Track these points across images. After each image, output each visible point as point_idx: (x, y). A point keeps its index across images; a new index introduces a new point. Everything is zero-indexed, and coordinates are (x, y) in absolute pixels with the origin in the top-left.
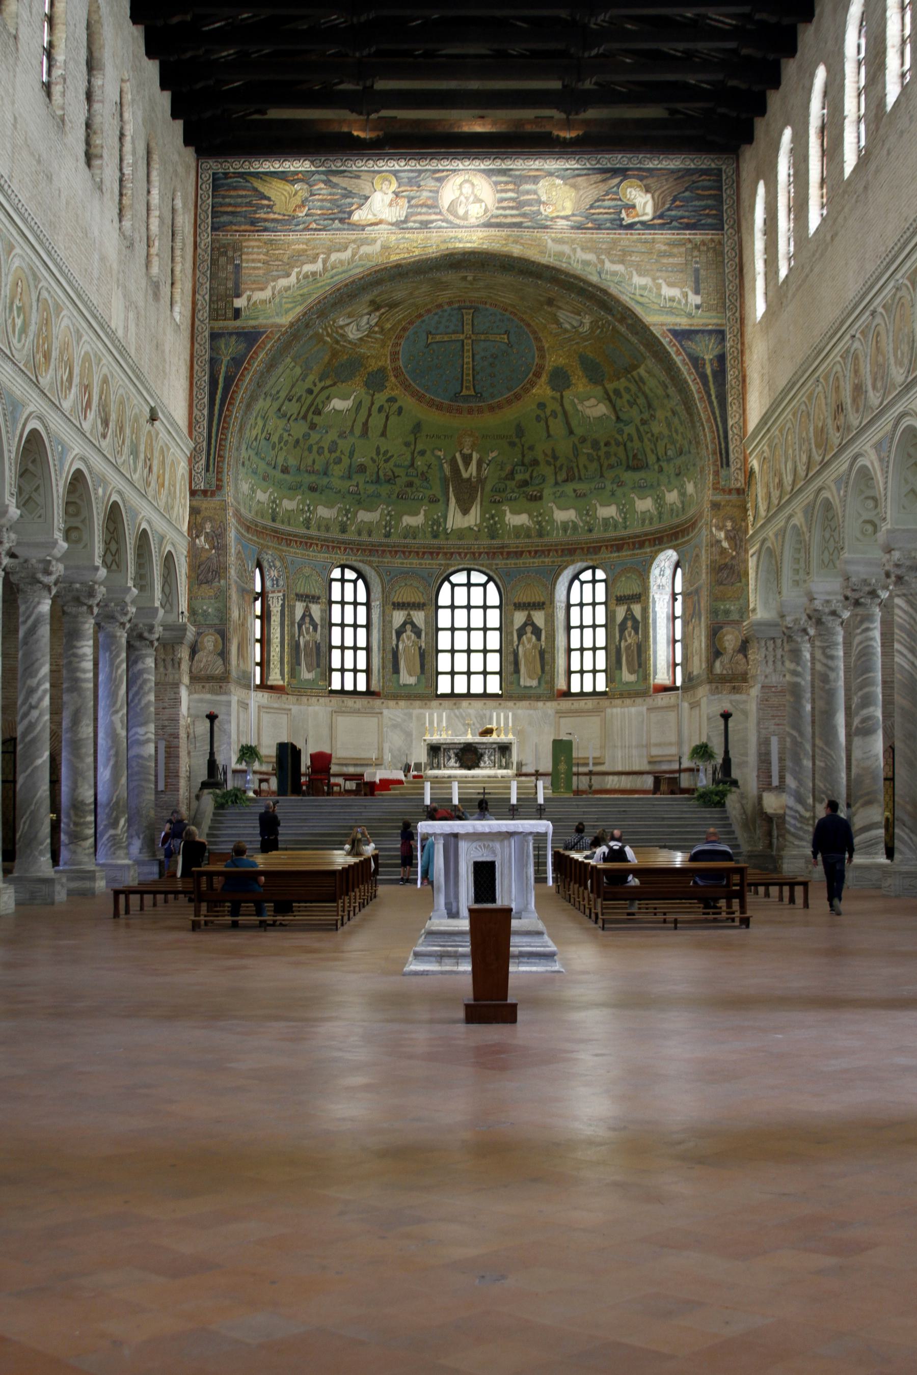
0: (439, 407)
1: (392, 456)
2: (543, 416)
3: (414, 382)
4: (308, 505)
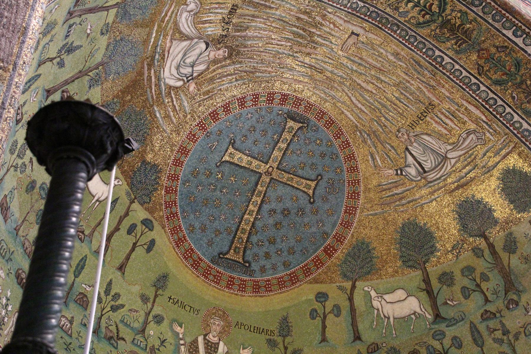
0: (196, 264)
1: (123, 306)
2: (320, 312)
3: (183, 211)
4: (8, 300)
